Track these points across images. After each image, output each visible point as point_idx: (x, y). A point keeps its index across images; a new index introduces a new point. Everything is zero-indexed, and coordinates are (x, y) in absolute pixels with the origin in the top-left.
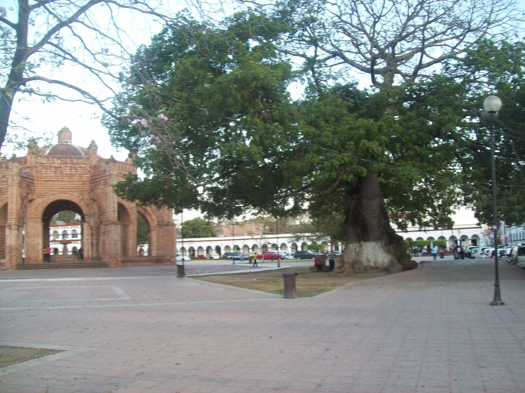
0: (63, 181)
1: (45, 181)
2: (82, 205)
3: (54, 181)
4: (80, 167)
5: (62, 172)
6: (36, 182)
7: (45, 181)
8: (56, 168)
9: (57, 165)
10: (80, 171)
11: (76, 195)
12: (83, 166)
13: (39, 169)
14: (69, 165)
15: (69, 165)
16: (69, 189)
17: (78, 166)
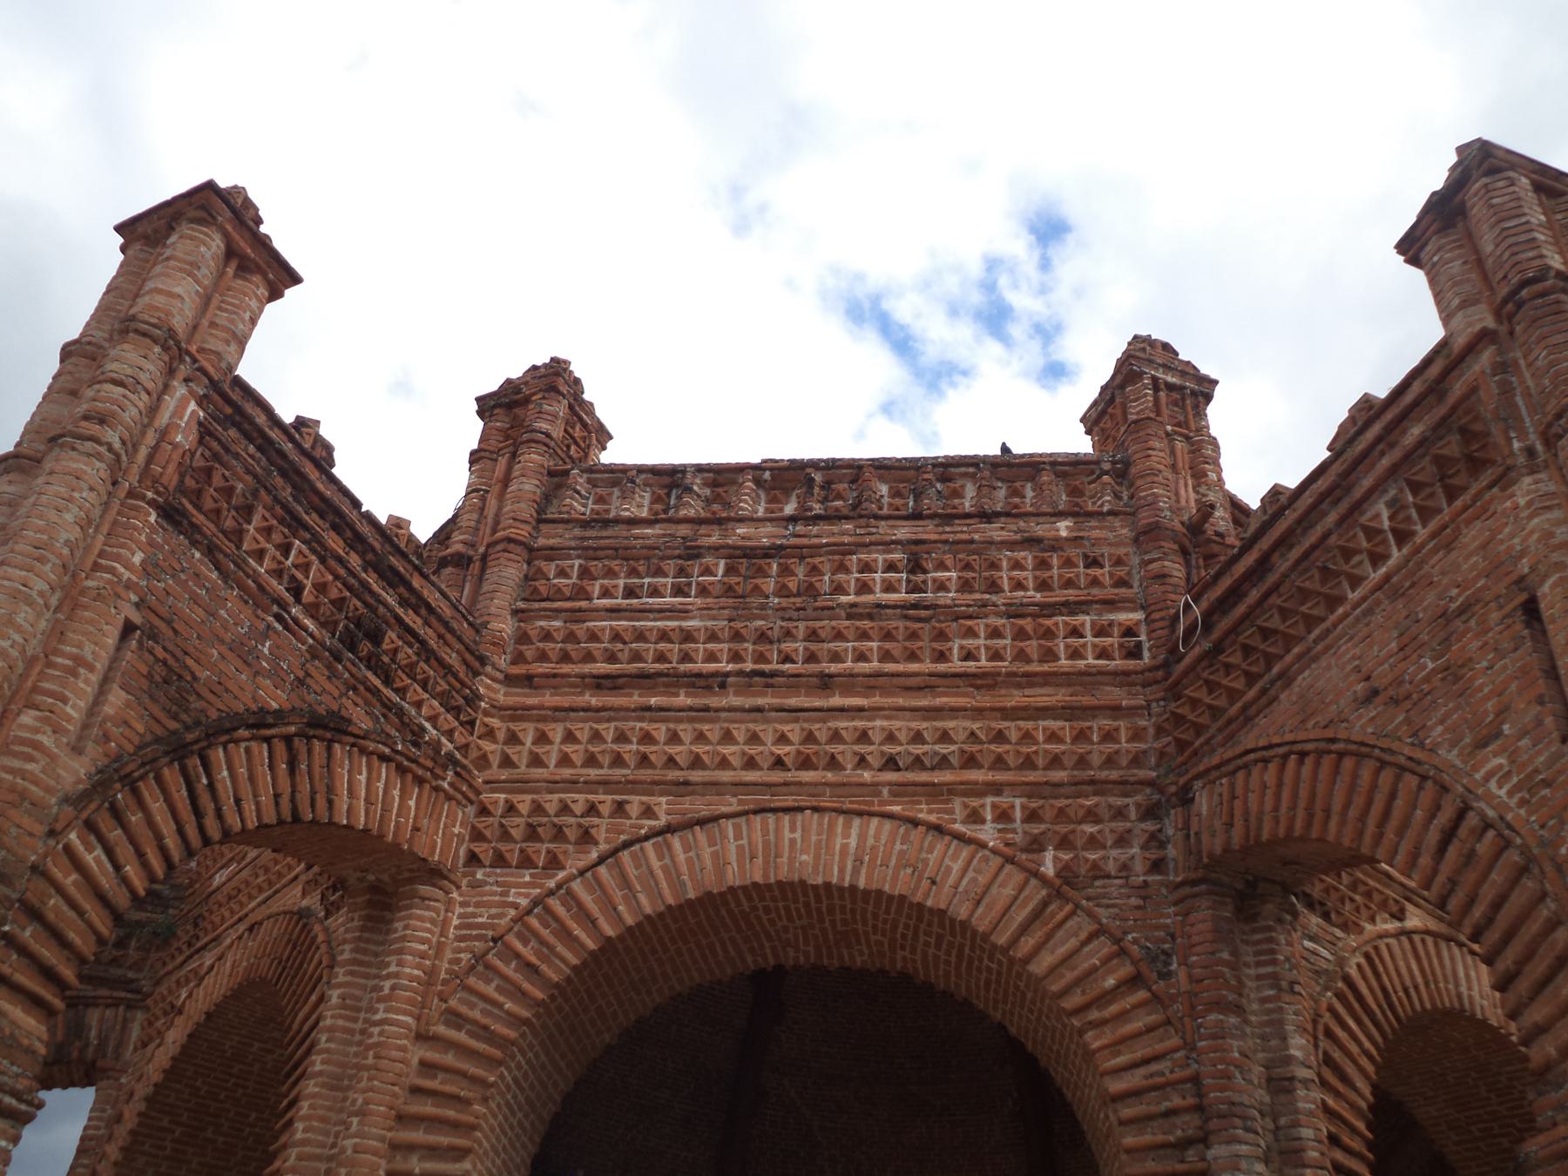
0: (826, 683)
1: (601, 683)
2: (1066, 956)
3: (700, 682)
4: (1031, 542)
5: (810, 591)
6: (487, 687)
7: (601, 683)
8: (749, 557)
9: (765, 535)
10: (1018, 580)
11: (988, 833)
12: (1063, 528)
13: (562, 576)
14: (903, 532)
15: (903, 532)
16: (891, 763)
17: (996, 531)
